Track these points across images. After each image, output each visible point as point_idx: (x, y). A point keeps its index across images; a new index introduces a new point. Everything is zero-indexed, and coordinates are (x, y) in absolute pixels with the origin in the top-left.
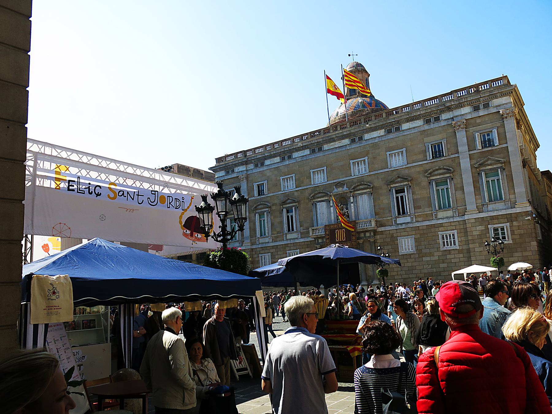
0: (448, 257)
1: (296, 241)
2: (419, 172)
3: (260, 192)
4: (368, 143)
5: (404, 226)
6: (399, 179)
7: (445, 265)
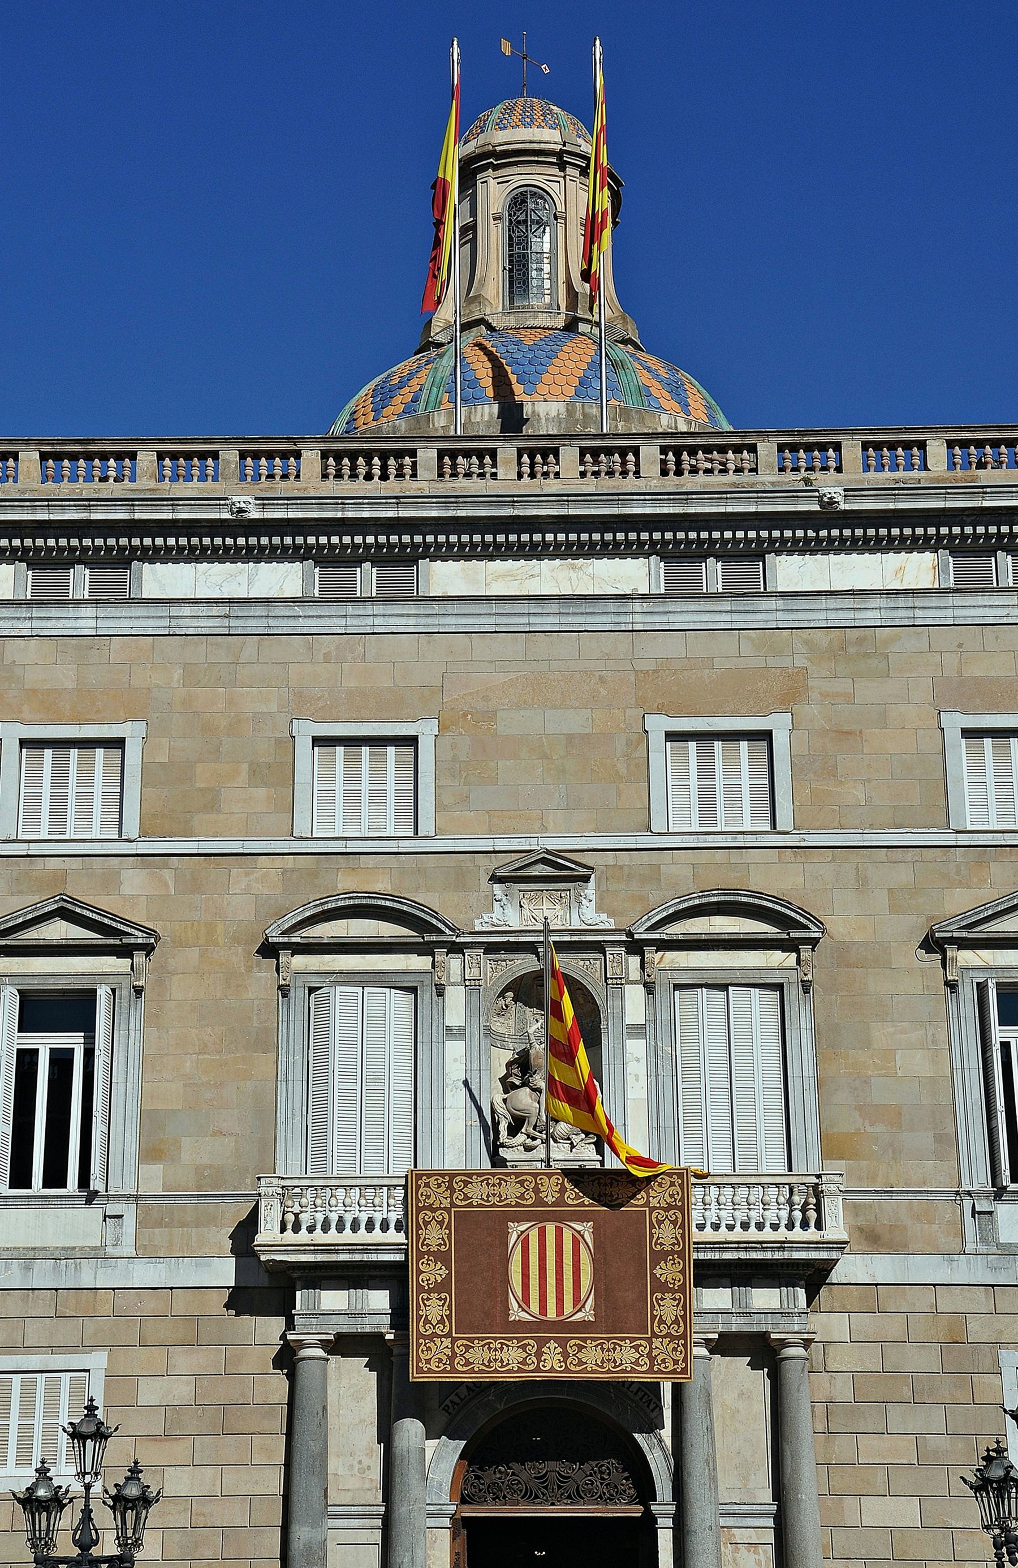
1: (88, 1276)
4: (802, 618)
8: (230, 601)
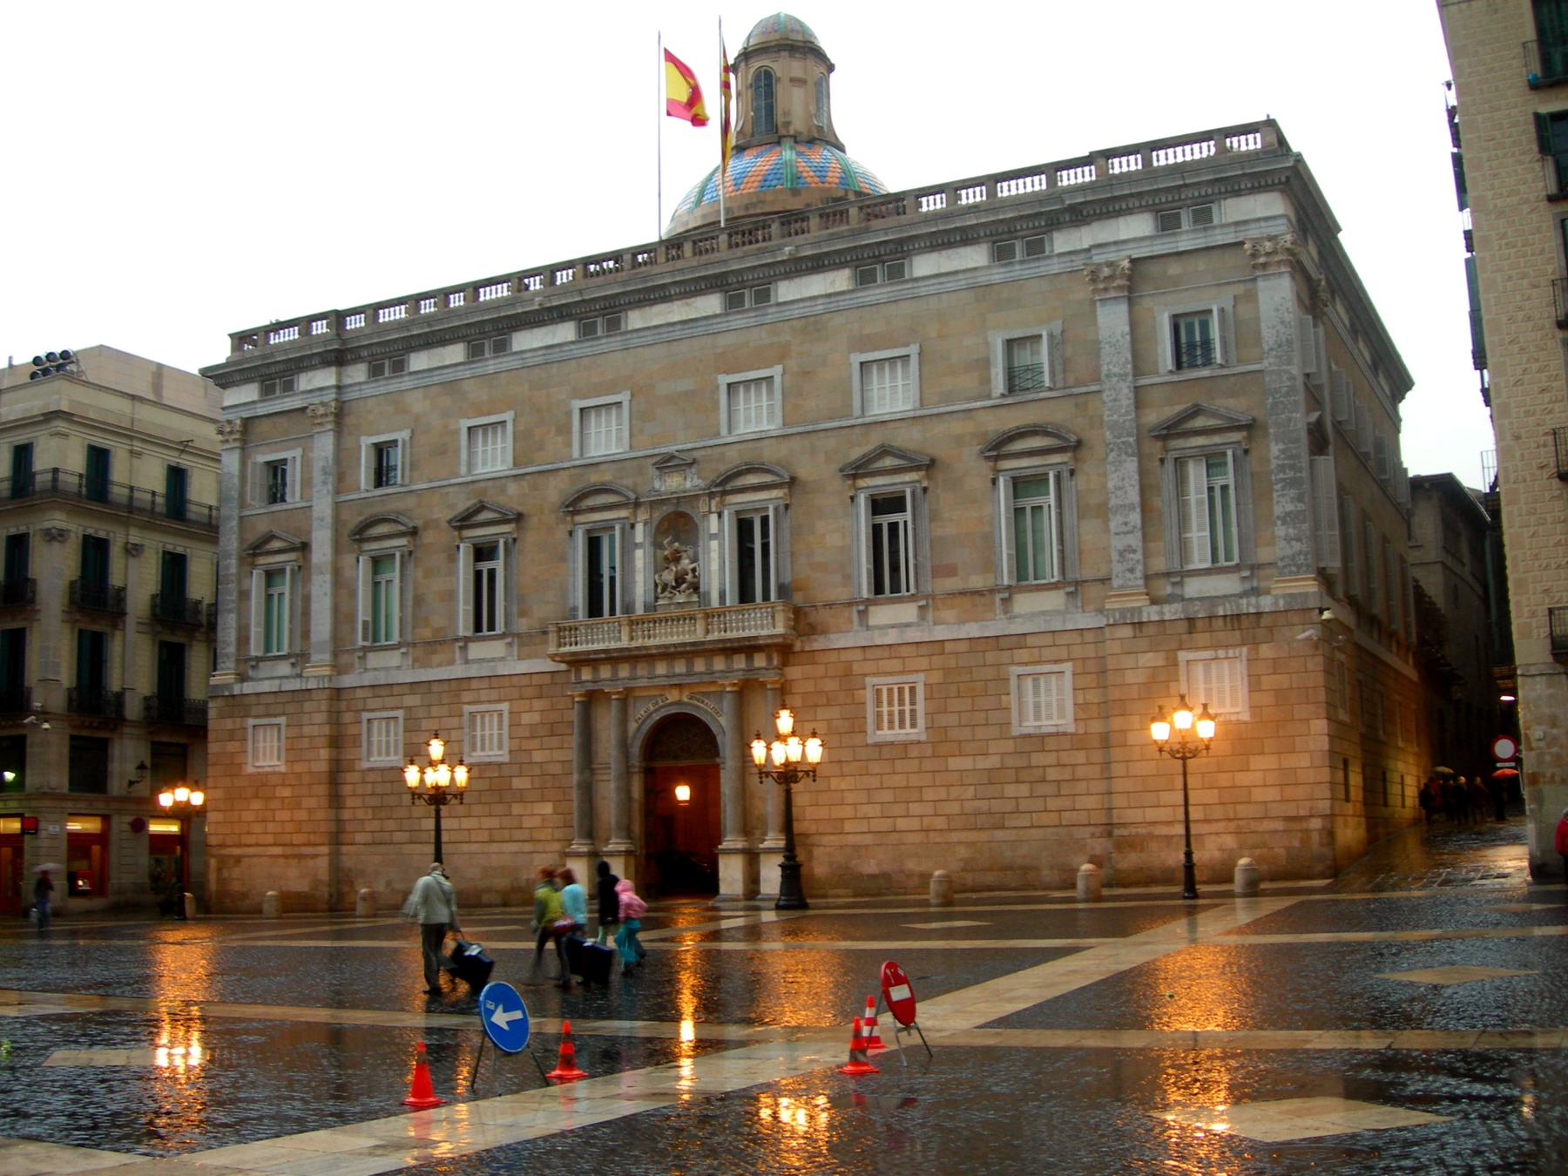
0: (1038, 759)
2: (959, 440)
3: (382, 476)
5: (891, 637)
6: (888, 462)
7: (1024, 790)
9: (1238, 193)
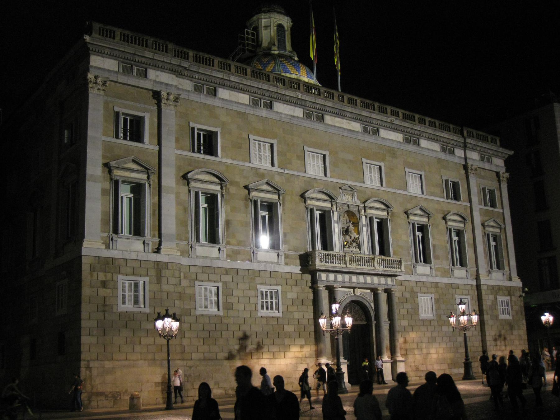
5: (424, 279)
6: (419, 212)
8: (292, 116)
9: (496, 156)
